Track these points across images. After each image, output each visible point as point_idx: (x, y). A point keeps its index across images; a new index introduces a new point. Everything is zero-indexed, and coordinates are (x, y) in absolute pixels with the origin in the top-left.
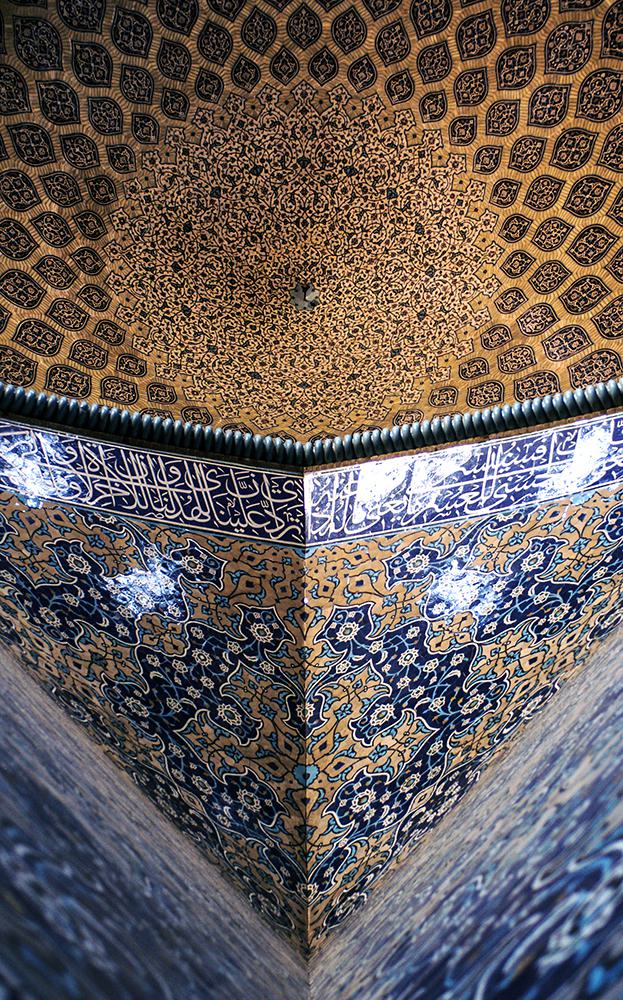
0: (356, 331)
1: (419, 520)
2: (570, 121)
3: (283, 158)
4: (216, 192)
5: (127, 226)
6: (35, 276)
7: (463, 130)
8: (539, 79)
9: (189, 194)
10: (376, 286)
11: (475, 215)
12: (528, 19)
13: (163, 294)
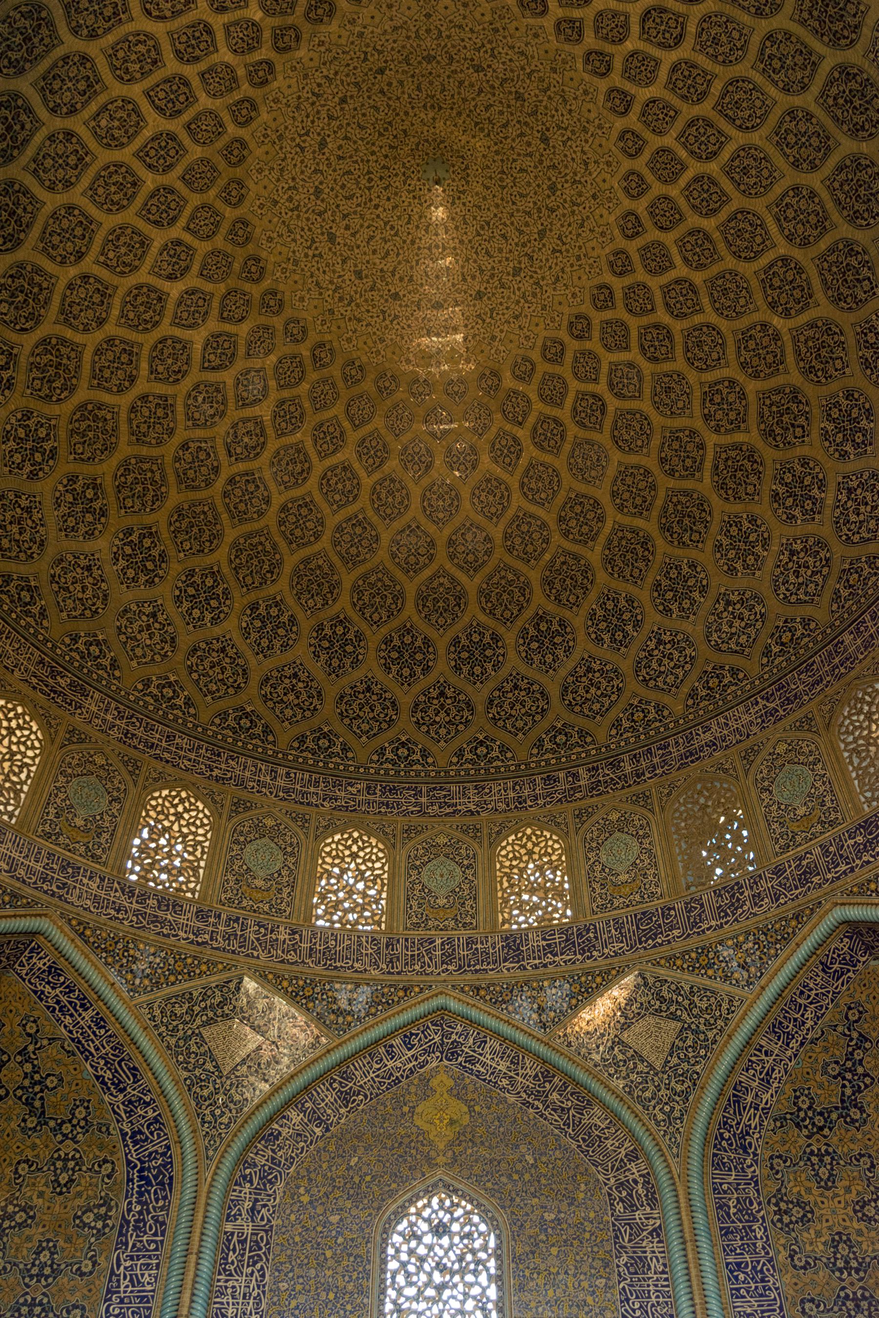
0: (437, 247)
1: (48, 1008)
2: (678, 327)
3: (505, 80)
4: (429, 59)
5: (323, 49)
6: (196, 82)
7: (632, 226)
8: (698, 278)
9: (403, 47)
10: (482, 228)
11: (575, 278)
12: (739, 242)
13: (313, 122)
